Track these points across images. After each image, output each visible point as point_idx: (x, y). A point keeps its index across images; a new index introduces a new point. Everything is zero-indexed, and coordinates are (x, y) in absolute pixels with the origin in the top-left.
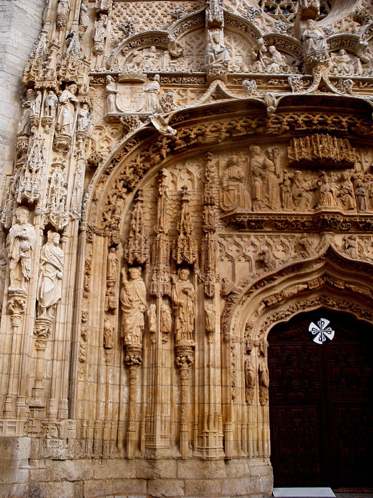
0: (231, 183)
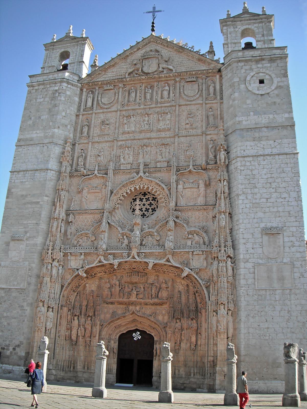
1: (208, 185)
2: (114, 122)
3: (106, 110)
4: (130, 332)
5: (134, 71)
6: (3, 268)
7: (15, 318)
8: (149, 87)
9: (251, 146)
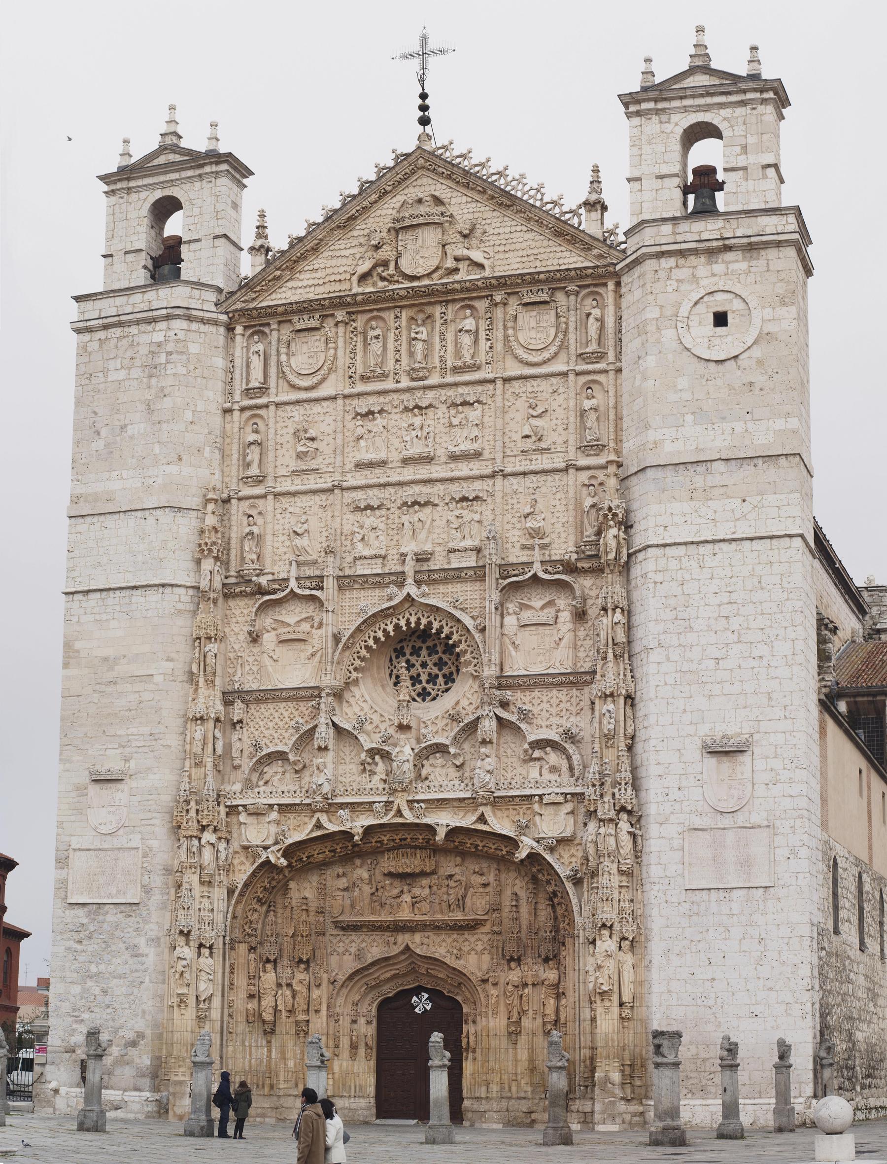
0: (339, 893)
1: (580, 615)
2: (329, 430)
3: (303, 395)
4: (406, 995)
5: (374, 267)
6: (78, 853)
7: (120, 978)
8: (420, 322)
9: (684, 515)
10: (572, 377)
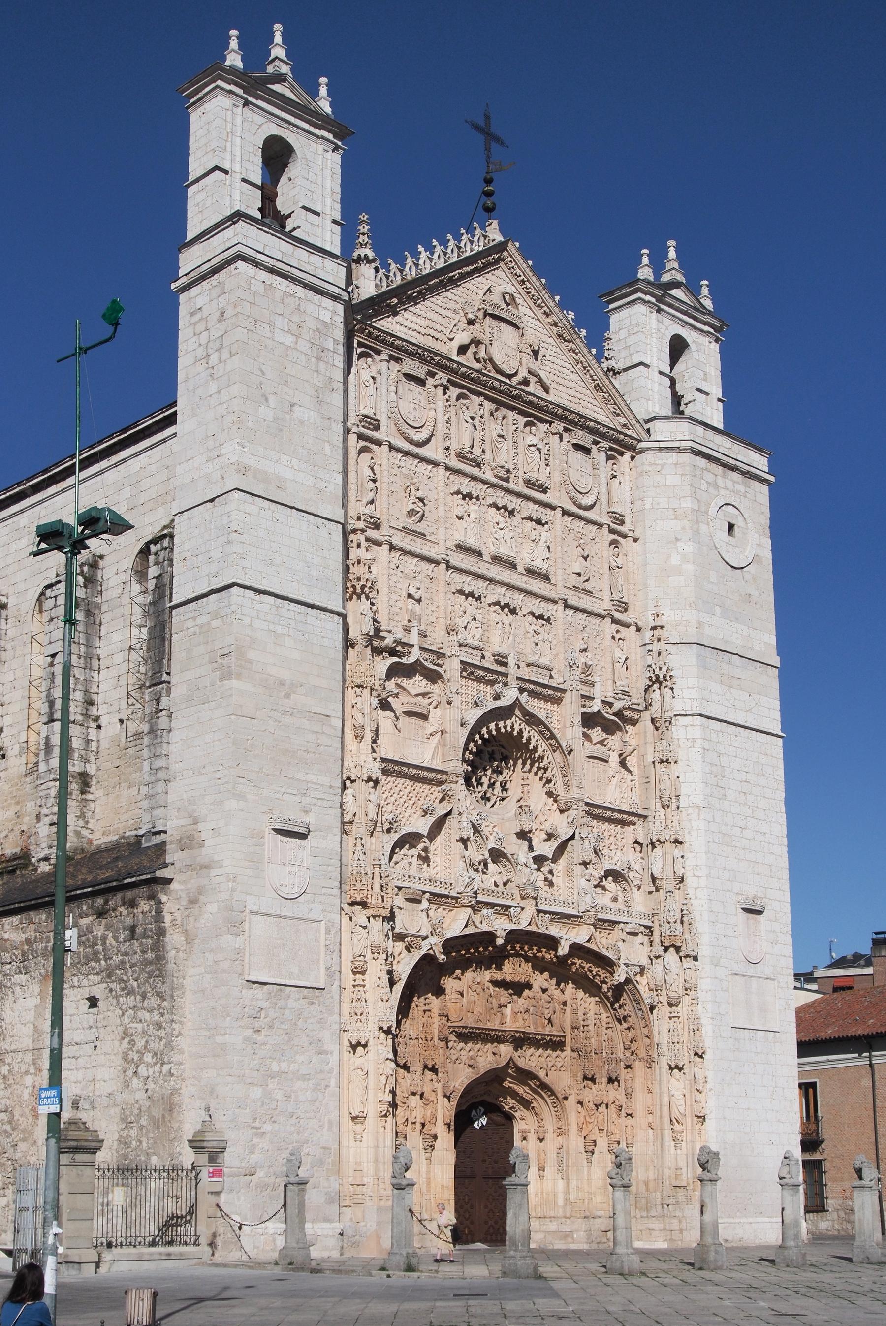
6: (256, 918)
7: (305, 1078)
9: (718, 695)
10: (606, 528)
